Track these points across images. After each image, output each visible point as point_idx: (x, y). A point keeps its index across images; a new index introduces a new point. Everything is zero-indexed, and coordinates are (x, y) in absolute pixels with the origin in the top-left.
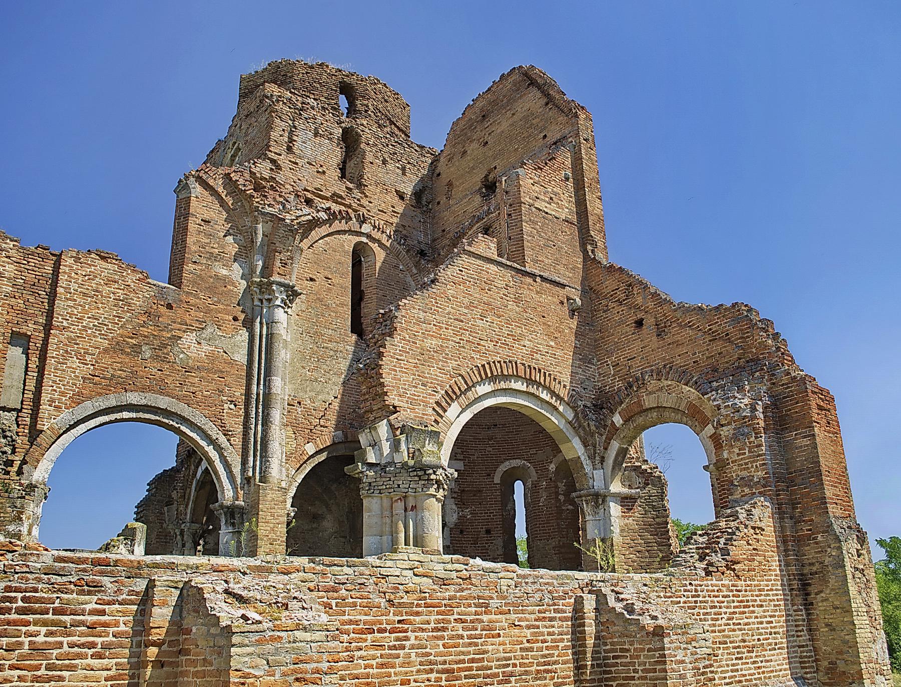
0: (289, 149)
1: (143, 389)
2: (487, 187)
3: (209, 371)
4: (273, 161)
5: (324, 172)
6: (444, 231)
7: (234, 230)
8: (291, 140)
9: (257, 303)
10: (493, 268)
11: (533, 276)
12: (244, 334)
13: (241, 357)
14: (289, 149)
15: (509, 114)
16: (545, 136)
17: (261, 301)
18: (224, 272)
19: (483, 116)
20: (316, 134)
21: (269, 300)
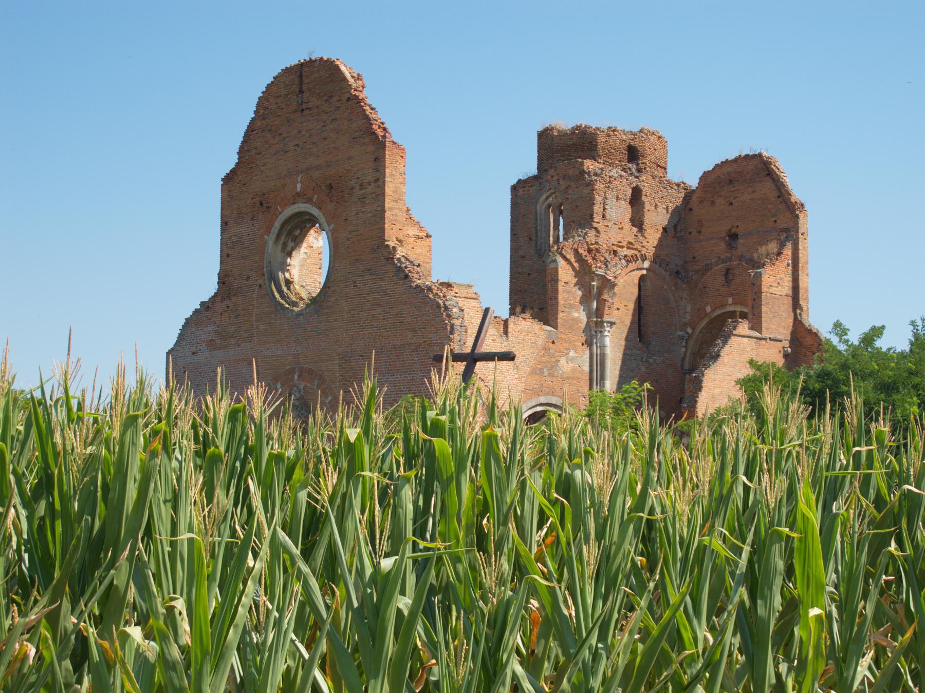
0: (604, 216)
1: (547, 394)
2: (729, 236)
3: (572, 378)
4: (596, 228)
5: (622, 228)
7: (580, 284)
8: (604, 209)
9: (593, 333)
10: (746, 340)
11: (765, 339)
12: (587, 352)
13: (586, 368)
14: (604, 216)
15: (750, 190)
16: (775, 221)
18: (576, 315)
20: (618, 199)
21: (601, 332)
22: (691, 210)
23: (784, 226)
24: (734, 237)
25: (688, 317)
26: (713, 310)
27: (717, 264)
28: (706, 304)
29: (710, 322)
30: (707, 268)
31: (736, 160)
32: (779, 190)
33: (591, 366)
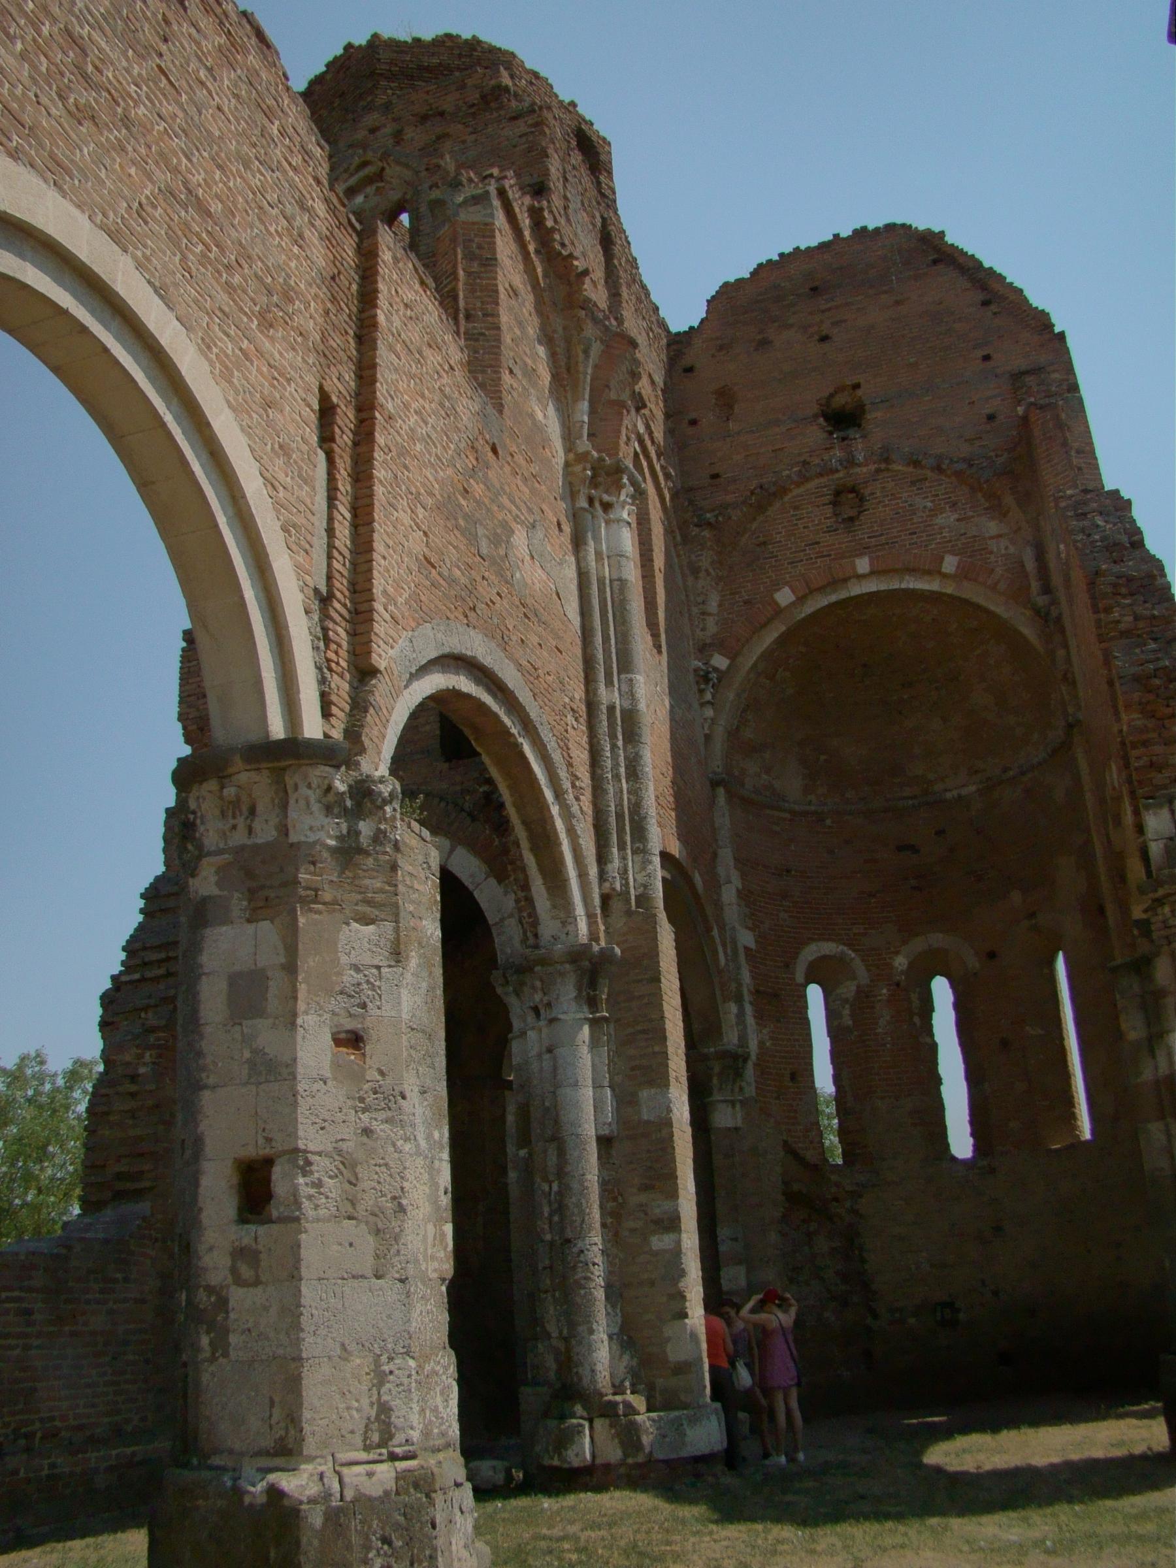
2: (827, 419)
6: (715, 476)
9: (583, 503)
16: (987, 358)
17: (591, 500)
19: (814, 289)
21: (607, 507)
22: (689, 370)
23: (1022, 364)
24: (843, 419)
25: (712, 627)
26: (801, 600)
27: (804, 479)
28: (776, 586)
29: (783, 640)
30: (766, 497)
31: (823, 246)
32: (984, 288)
33: (585, 612)
